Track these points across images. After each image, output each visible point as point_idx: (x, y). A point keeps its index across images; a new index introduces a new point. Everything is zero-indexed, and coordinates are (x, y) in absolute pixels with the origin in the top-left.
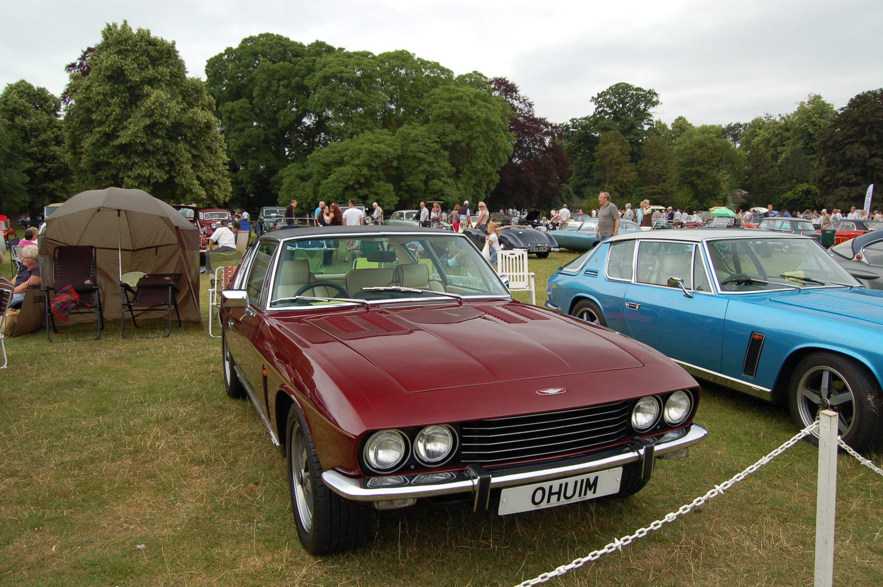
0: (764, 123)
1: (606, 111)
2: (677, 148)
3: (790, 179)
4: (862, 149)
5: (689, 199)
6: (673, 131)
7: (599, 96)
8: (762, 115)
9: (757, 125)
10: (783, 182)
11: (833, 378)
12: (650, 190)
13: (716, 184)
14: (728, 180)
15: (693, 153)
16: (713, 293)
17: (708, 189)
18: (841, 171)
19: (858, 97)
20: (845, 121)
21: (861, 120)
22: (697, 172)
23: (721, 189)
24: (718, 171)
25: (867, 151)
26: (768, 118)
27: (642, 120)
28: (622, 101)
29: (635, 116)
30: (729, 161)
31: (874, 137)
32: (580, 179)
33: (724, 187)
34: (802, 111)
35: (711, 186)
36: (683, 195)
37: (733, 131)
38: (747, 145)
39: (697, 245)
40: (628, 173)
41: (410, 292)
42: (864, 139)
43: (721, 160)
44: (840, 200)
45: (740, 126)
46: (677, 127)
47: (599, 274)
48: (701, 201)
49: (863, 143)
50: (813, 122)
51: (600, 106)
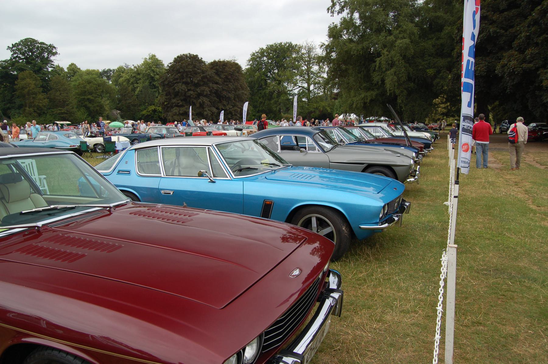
0: (124, 69)
1: (20, 57)
2: (73, 83)
3: (144, 103)
4: (183, 86)
5: (85, 116)
6: (68, 73)
7: (14, 46)
8: (123, 65)
9: (121, 71)
10: (140, 105)
11: (318, 219)
12: (59, 111)
13: (101, 107)
14: (108, 104)
15: (85, 87)
16: (229, 178)
17: (97, 110)
18: (174, 98)
19: (178, 57)
20: (173, 70)
21: (181, 70)
22: (88, 99)
23: (105, 110)
24: (102, 99)
25: (186, 88)
26: (127, 66)
27: (47, 64)
28: (31, 50)
29: (41, 61)
30: (107, 92)
31: (189, 80)
32: (5, 105)
33: (106, 108)
34: (146, 63)
35: (98, 108)
36: (79, 114)
37: (106, 73)
38: (116, 82)
39: (208, 148)
40: (42, 100)
41: (66, 208)
42: (184, 80)
43: (102, 92)
44: (174, 115)
45: (111, 71)
46: (71, 70)
47: (132, 172)
48: (93, 117)
49: (183, 83)
50: (153, 70)
51: (15, 53)
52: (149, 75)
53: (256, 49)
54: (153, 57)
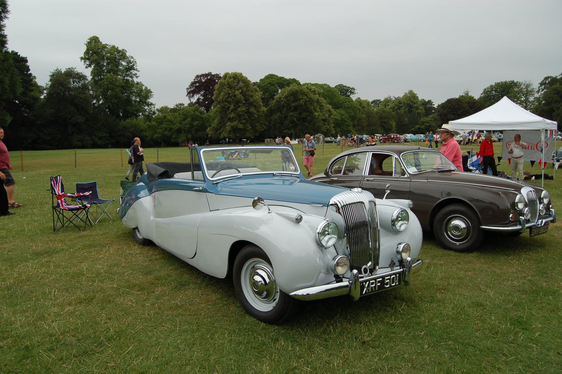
9: (387, 101)
13: (391, 125)
52: (408, 104)
53: (487, 85)
54: (411, 92)
